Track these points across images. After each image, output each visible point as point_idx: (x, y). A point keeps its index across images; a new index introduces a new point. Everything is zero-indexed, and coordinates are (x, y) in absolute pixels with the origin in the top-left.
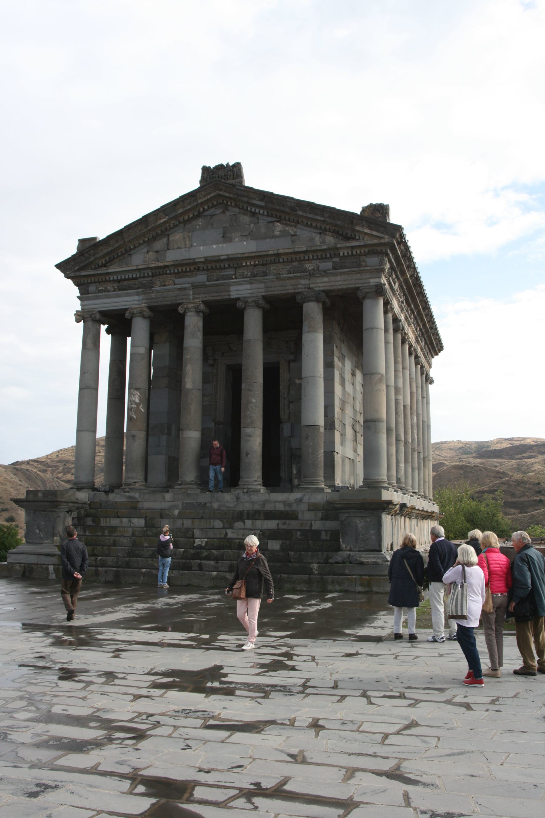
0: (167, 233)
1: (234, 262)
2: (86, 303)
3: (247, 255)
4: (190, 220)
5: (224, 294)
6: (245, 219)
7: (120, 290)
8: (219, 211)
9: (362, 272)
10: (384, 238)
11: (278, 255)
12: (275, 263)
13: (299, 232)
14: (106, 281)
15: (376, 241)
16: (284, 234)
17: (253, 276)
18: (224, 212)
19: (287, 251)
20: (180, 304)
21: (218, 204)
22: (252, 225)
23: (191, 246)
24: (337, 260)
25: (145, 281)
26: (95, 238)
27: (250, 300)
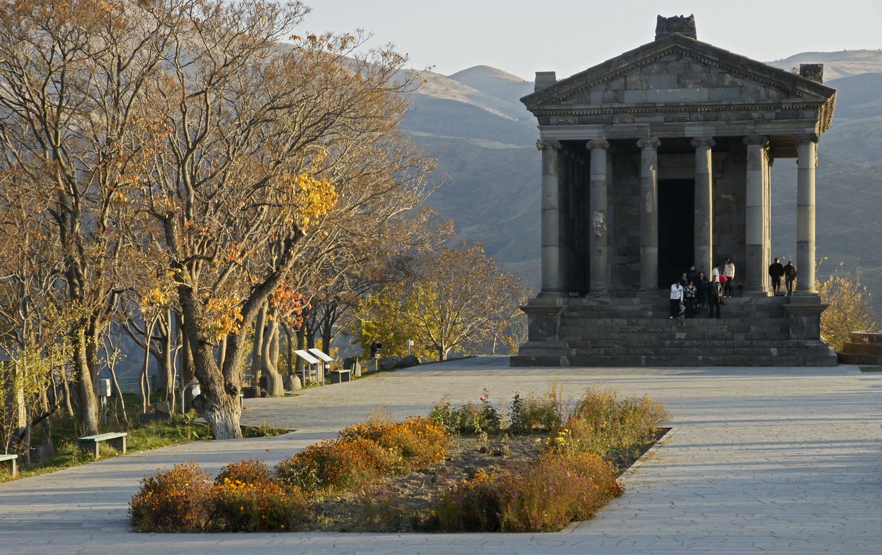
1: (691, 108)
2: (545, 132)
4: (647, 65)
6: (697, 68)
7: (580, 123)
9: (799, 122)
11: (730, 105)
13: (746, 84)
16: (733, 85)
17: (706, 120)
18: (678, 60)
20: (638, 139)
22: (704, 75)
24: (779, 111)
26: (553, 73)
27: (703, 140)
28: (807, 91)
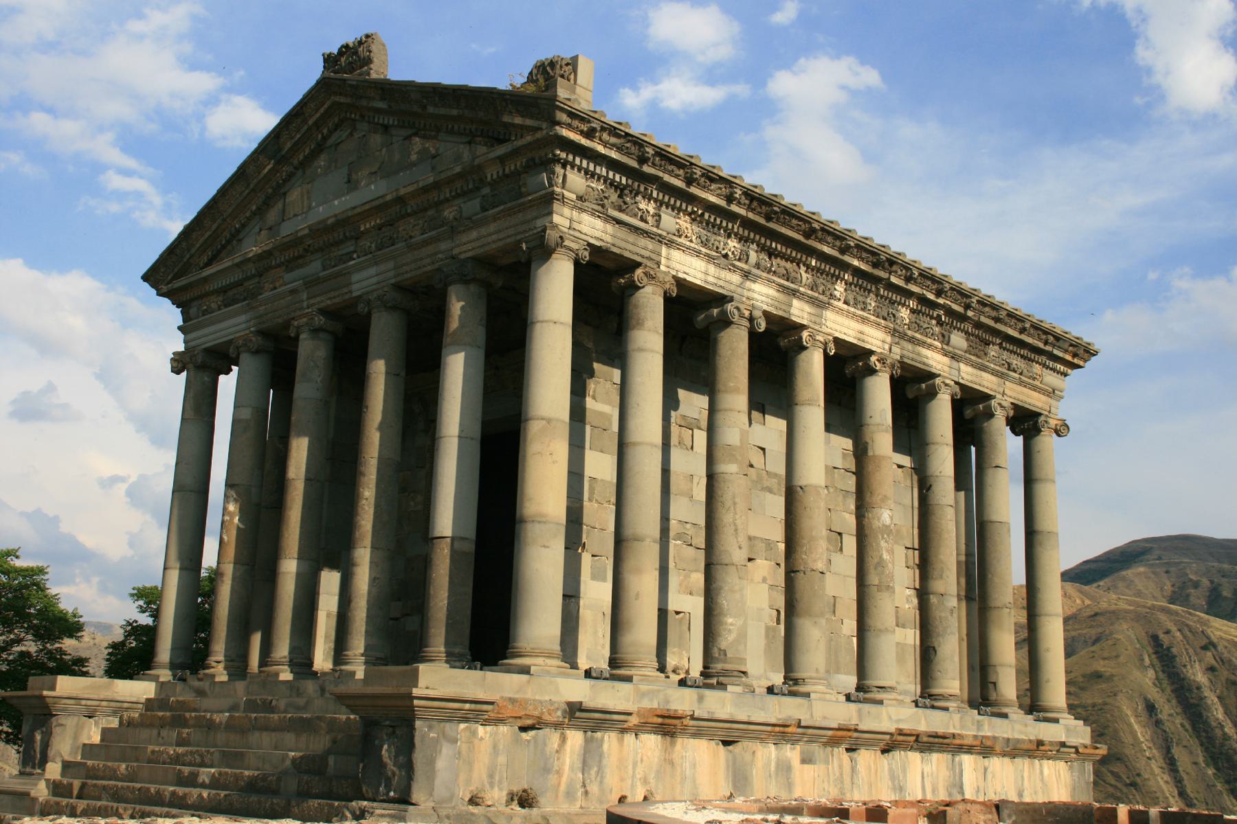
0: (282, 191)
3: (359, 210)
5: (345, 290)
6: (377, 139)
7: (226, 306)
8: (342, 134)
10: (541, 129)
11: (400, 200)
12: (403, 217)
14: (207, 295)
15: (529, 138)
18: (351, 134)
19: (410, 189)
21: (342, 121)
23: (310, 208)
24: (486, 191)
25: (250, 284)
28: (518, 120)
